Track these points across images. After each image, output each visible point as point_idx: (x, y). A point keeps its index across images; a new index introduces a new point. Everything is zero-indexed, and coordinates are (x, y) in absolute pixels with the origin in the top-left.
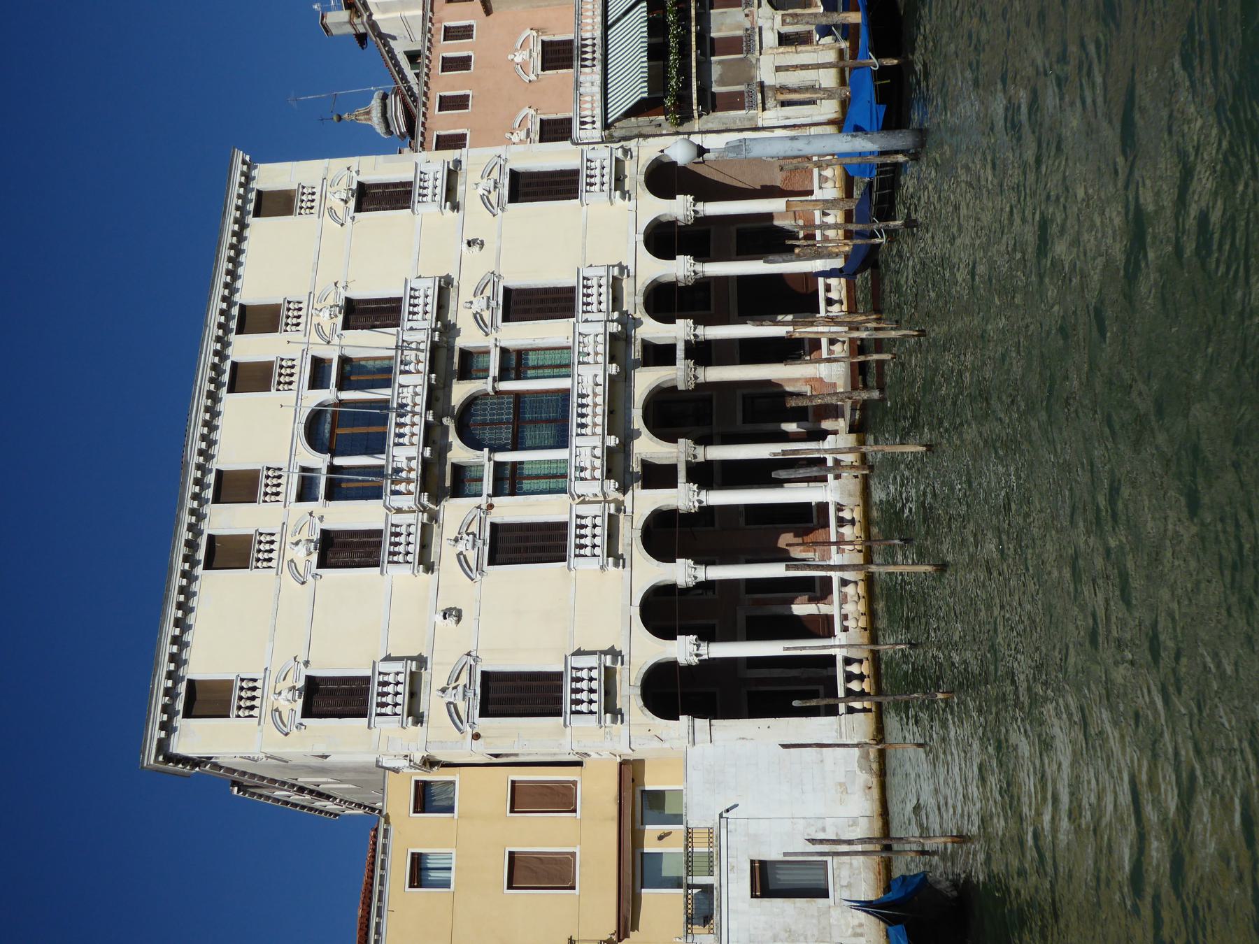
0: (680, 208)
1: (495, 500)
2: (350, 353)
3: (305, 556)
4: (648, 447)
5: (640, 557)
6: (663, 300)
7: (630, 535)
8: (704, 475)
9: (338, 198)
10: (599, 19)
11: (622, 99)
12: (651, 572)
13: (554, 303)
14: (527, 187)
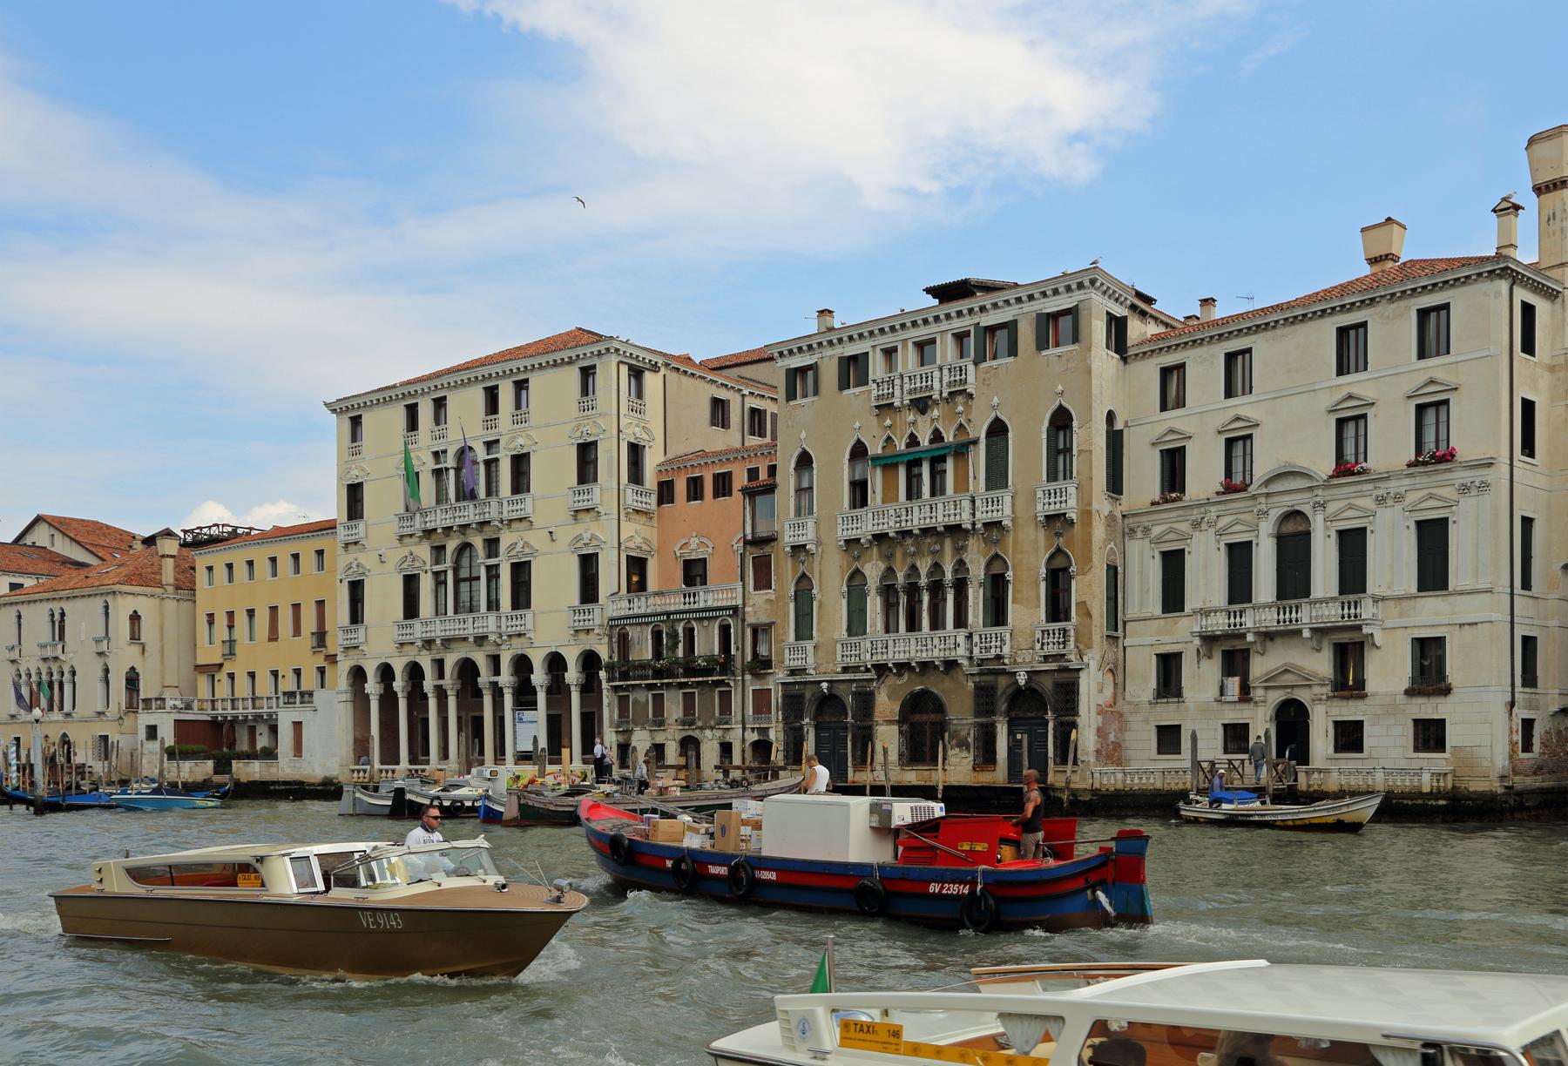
0: (573, 676)
4: (451, 661)
5: (405, 660)
7: (412, 654)
9: (590, 432)
10: (672, 608)
12: (399, 667)
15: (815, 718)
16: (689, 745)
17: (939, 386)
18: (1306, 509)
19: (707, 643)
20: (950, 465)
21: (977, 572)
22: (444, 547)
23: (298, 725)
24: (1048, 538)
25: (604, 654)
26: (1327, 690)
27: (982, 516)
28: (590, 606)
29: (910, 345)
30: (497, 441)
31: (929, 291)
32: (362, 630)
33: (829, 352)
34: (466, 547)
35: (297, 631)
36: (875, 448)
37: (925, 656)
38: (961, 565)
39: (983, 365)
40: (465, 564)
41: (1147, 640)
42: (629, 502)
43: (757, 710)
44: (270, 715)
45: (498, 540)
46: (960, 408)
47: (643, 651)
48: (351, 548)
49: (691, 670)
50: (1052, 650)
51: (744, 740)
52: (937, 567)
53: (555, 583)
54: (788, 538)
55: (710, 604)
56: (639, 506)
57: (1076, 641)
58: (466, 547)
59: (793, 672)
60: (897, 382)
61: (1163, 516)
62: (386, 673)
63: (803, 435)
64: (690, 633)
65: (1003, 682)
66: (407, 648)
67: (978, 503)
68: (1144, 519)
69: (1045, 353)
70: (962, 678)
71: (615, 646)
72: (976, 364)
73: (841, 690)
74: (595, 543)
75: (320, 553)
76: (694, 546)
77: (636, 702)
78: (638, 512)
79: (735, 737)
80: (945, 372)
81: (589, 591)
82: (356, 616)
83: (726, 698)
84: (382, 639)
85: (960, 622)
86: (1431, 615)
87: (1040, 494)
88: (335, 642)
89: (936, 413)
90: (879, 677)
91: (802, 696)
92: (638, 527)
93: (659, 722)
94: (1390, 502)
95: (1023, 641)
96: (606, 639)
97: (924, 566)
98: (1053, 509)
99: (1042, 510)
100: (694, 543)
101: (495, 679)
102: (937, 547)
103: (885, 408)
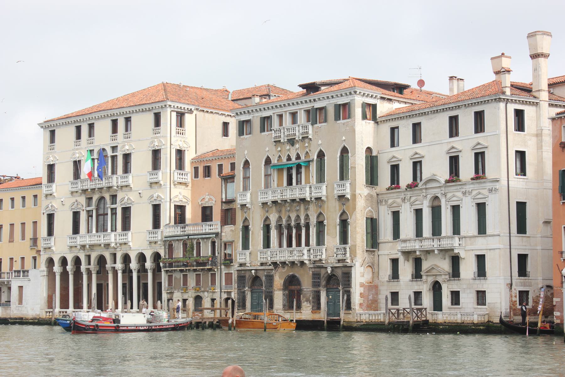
0: (149, 264)
1: (85, 211)
2: (118, 157)
4: (94, 256)
9: (156, 145)
10: (191, 232)
15: (251, 287)
16: (198, 299)
17: (298, 133)
18: (439, 195)
19: (206, 251)
20: (303, 170)
21: (313, 221)
22: (92, 198)
23: (21, 288)
24: (340, 206)
25: (162, 255)
26: (447, 277)
27: (314, 195)
28: (156, 230)
29: (288, 114)
30: (117, 146)
31: (300, 86)
32: (53, 238)
33: (256, 114)
34: (102, 199)
35: (23, 238)
36: (274, 161)
37: (291, 259)
38: (307, 217)
39: (316, 126)
40: (103, 209)
41: (386, 252)
42: (176, 179)
43: (226, 284)
44: (8, 282)
45: (116, 195)
46: (307, 145)
47: (179, 253)
48: (49, 197)
49: (199, 264)
50: (340, 257)
51: (221, 298)
52: (298, 217)
53: (141, 219)
54: (239, 201)
55: (207, 231)
56: (181, 181)
57: (350, 253)
58: (102, 199)
59: (241, 265)
60: (282, 131)
61: (392, 195)
62: (64, 261)
63: (246, 152)
64: (198, 244)
65: (323, 271)
66: (74, 249)
67: (313, 188)
68: (385, 196)
69: (338, 122)
70: (308, 269)
71: (167, 250)
72: (312, 125)
73: (260, 274)
74: (159, 199)
75: (35, 196)
76: (207, 200)
77: (176, 278)
78: (180, 183)
79: (217, 296)
80: (301, 127)
81: (156, 224)
82: (50, 232)
83: (213, 276)
84: (62, 245)
85: (307, 244)
86: (481, 245)
87: (336, 186)
88: (41, 244)
89: (297, 146)
90: (275, 268)
91: (244, 277)
92: (180, 190)
93: (185, 288)
94: (467, 195)
95: (329, 252)
96: (163, 247)
97: (293, 216)
98: (341, 193)
99: (337, 192)
100: (207, 198)
101: (114, 265)
102: (298, 208)
103: (277, 142)
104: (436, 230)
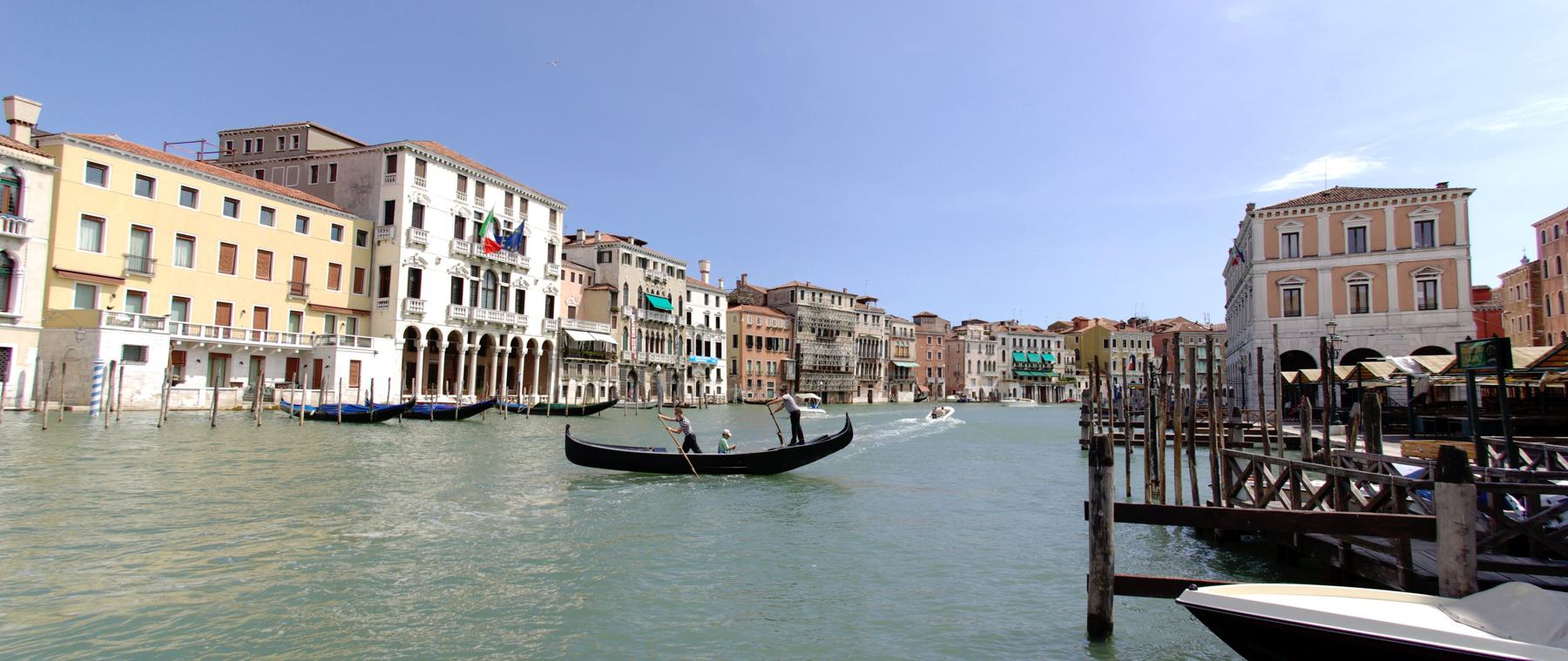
3: (459, 209)
6: (516, 342)
8: (469, 353)
11: (571, 333)
12: (445, 332)
13: (520, 308)
14: (550, 300)
53: (535, 304)
104: (708, 354)
